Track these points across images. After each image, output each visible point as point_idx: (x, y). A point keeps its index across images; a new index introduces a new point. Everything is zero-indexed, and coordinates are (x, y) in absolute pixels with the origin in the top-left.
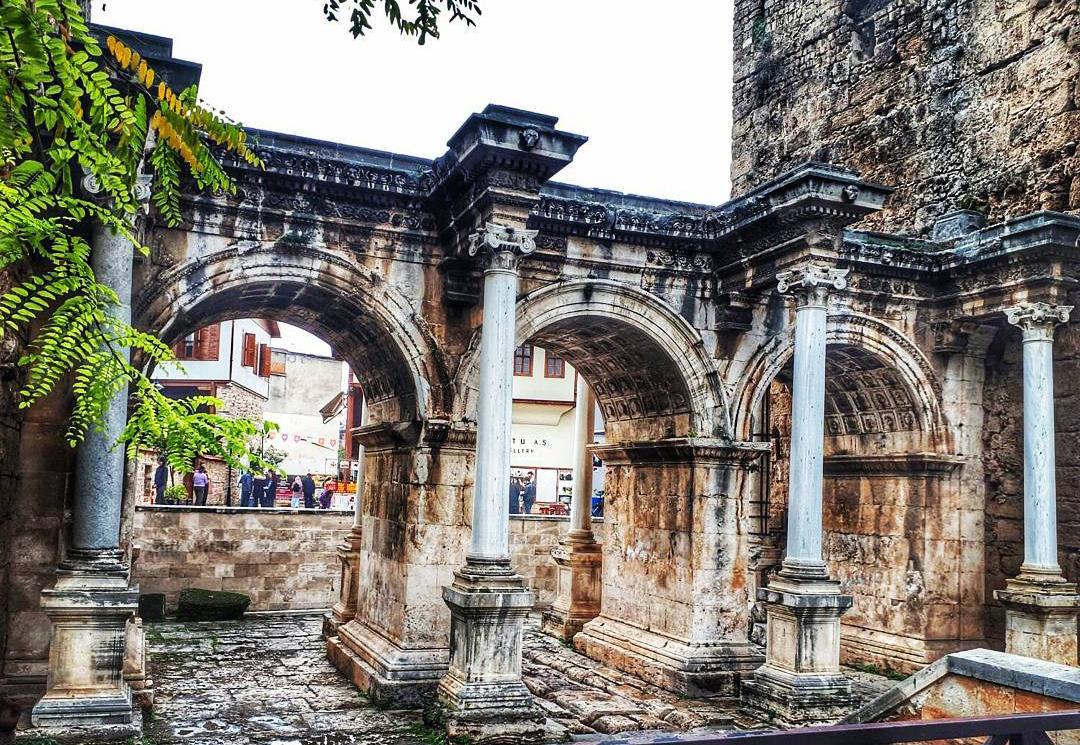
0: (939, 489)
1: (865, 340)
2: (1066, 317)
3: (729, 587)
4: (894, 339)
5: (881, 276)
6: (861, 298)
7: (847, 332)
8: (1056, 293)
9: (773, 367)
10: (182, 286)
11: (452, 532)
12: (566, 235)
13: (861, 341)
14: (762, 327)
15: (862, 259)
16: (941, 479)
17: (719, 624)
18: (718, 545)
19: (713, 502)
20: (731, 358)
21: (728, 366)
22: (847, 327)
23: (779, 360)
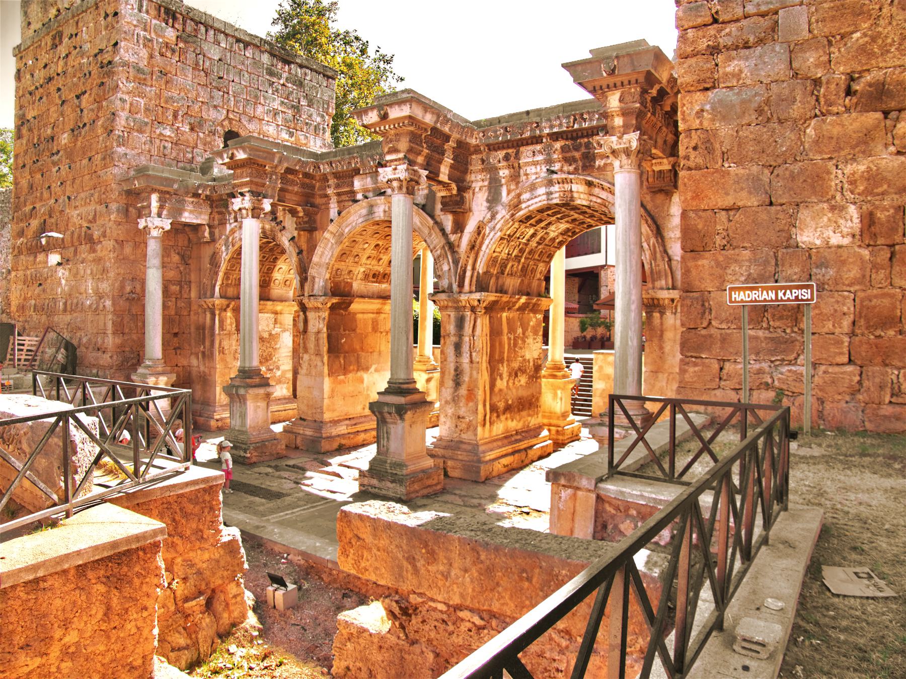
0: (662, 324)
1: (575, 195)
2: (635, 145)
3: (464, 401)
4: (603, 189)
5: (582, 137)
6: (568, 160)
7: (556, 192)
8: (621, 124)
9: (492, 234)
10: (223, 248)
11: (313, 357)
12: (353, 177)
13: (572, 197)
14: (485, 204)
15: (547, 131)
16: (662, 314)
17: (456, 426)
18: (456, 370)
19: (453, 339)
20: (462, 232)
21: (461, 238)
22: (556, 188)
23: (498, 226)
